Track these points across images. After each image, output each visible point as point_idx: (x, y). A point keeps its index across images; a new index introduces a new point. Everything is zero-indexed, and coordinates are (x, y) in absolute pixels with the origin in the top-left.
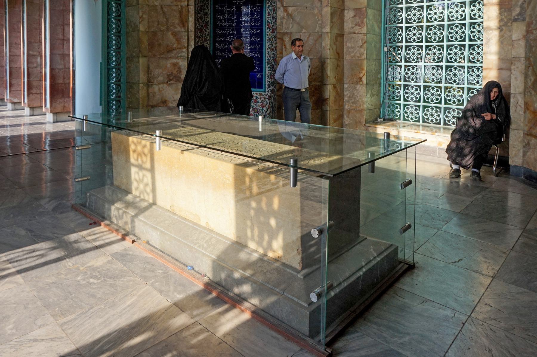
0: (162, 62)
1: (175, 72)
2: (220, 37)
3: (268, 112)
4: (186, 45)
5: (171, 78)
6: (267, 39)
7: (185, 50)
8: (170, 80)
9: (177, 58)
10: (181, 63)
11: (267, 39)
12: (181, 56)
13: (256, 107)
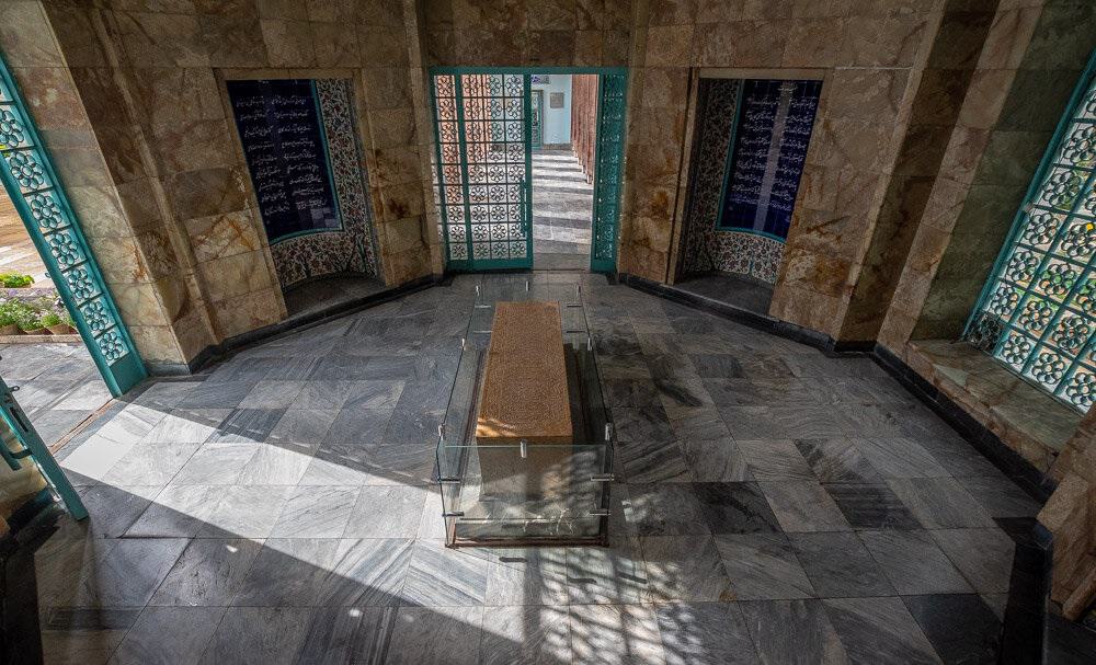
7: (676, 176)
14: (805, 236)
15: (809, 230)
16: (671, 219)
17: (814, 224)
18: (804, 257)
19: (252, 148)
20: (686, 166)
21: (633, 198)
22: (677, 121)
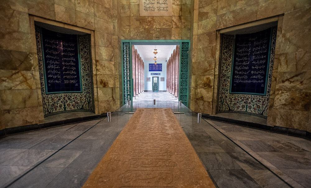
0: (202, 77)
1: (207, 82)
2: (239, 62)
3: (266, 109)
4: (214, 68)
5: (206, 85)
6: (271, 61)
7: (213, 70)
8: (205, 86)
9: (209, 75)
10: (210, 78)
11: (271, 61)
12: (211, 74)
13: (259, 104)
14: (281, 84)
15: (283, 82)
16: (213, 87)
17: (285, 78)
18: (283, 94)
19: (48, 56)
20: (217, 66)
21: (196, 81)
22: (212, 50)
